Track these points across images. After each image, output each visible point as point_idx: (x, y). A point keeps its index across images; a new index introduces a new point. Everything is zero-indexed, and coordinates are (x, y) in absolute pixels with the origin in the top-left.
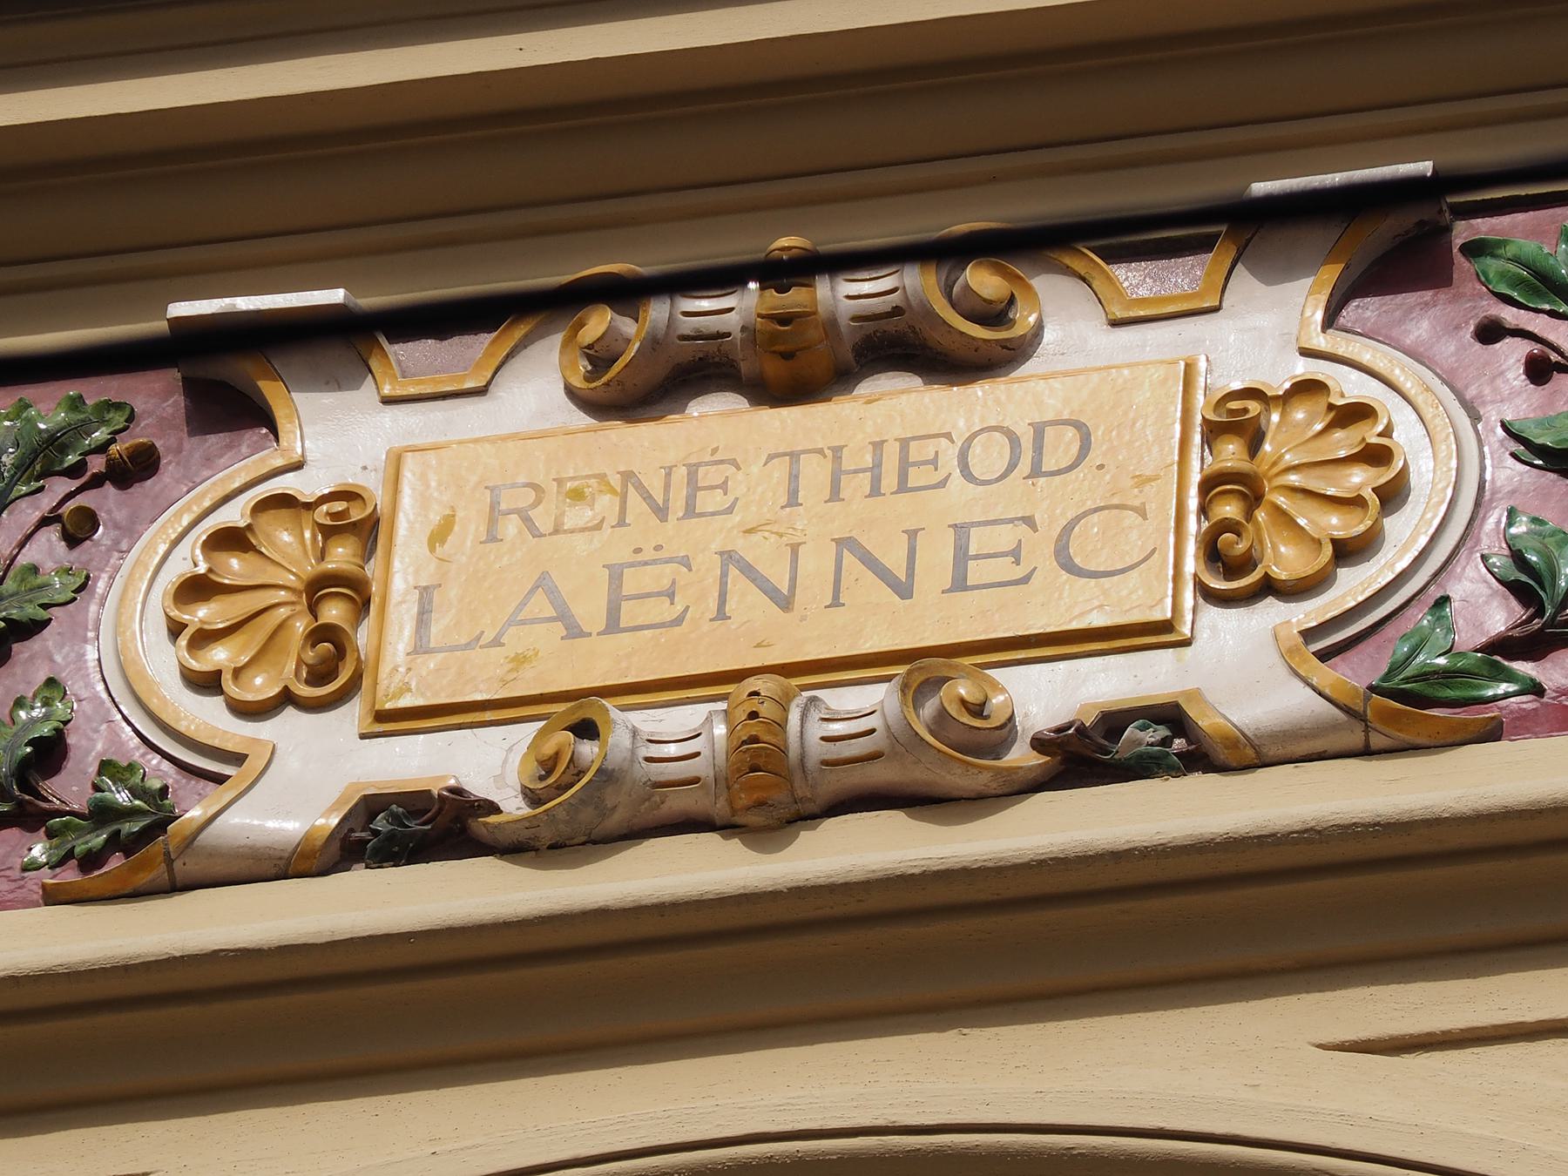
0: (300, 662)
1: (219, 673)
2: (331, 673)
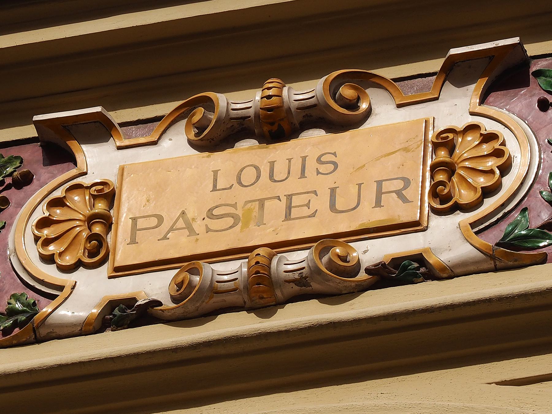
0: (85, 248)
1: (54, 254)
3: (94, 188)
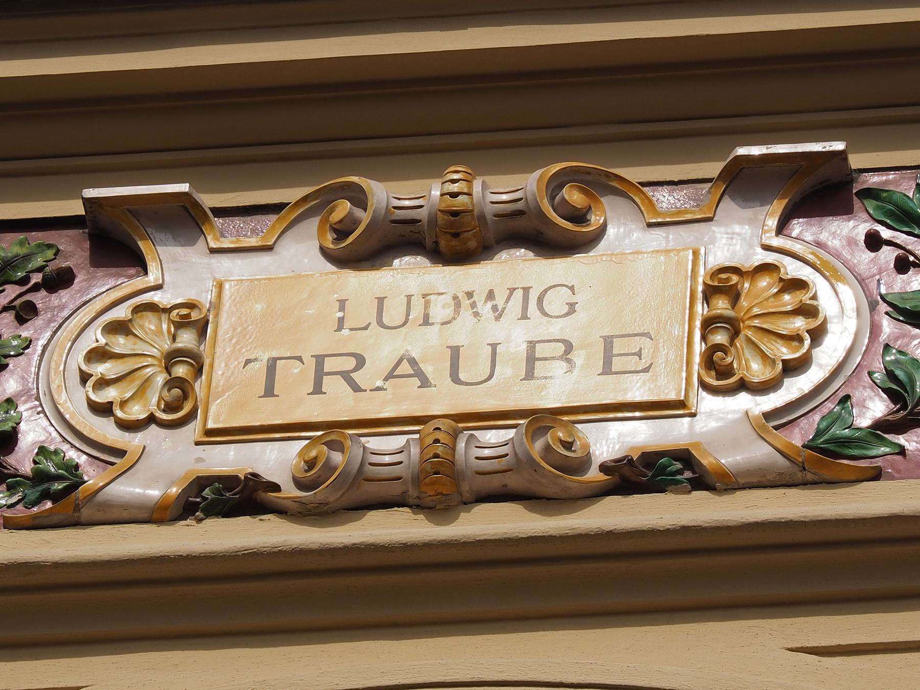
0: (161, 398)
1: (111, 403)
2: (179, 407)
3: (175, 312)
